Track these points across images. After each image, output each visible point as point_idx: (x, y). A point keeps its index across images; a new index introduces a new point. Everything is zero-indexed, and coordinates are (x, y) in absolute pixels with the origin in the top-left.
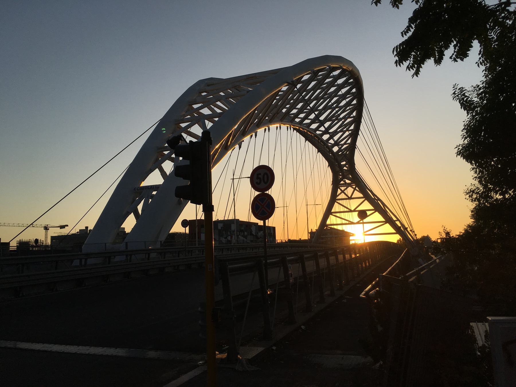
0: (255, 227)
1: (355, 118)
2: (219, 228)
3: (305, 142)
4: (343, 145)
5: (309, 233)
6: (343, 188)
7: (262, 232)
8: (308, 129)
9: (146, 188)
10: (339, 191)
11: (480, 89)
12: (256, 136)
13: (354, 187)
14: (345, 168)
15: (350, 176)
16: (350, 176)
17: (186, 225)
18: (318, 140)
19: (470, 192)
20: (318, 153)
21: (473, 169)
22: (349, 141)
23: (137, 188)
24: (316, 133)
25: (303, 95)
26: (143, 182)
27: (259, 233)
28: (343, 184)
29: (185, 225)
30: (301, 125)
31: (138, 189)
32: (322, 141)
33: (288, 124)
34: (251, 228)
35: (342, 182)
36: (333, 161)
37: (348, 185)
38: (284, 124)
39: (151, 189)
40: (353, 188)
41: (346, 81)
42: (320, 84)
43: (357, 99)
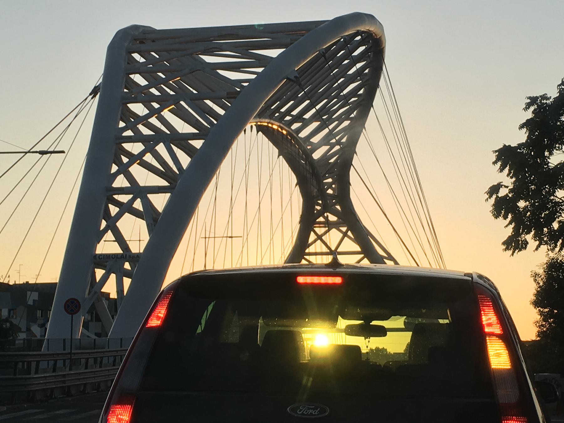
0: (107, 302)
1: (361, 98)
2: (30, 302)
3: (257, 135)
6: (320, 230)
8: (280, 122)
9: (113, 256)
10: (312, 237)
11: (544, 265)
13: (344, 229)
14: (330, 191)
15: (338, 207)
16: (338, 207)
18: (291, 140)
19: (536, 322)
20: (278, 157)
22: (344, 140)
23: (99, 257)
25: (303, 92)
26: (98, 245)
27: (115, 317)
28: (320, 223)
30: (271, 119)
32: (297, 140)
35: (321, 219)
36: (308, 175)
37: (329, 225)
39: (122, 259)
41: (362, 54)
43: (369, 69)
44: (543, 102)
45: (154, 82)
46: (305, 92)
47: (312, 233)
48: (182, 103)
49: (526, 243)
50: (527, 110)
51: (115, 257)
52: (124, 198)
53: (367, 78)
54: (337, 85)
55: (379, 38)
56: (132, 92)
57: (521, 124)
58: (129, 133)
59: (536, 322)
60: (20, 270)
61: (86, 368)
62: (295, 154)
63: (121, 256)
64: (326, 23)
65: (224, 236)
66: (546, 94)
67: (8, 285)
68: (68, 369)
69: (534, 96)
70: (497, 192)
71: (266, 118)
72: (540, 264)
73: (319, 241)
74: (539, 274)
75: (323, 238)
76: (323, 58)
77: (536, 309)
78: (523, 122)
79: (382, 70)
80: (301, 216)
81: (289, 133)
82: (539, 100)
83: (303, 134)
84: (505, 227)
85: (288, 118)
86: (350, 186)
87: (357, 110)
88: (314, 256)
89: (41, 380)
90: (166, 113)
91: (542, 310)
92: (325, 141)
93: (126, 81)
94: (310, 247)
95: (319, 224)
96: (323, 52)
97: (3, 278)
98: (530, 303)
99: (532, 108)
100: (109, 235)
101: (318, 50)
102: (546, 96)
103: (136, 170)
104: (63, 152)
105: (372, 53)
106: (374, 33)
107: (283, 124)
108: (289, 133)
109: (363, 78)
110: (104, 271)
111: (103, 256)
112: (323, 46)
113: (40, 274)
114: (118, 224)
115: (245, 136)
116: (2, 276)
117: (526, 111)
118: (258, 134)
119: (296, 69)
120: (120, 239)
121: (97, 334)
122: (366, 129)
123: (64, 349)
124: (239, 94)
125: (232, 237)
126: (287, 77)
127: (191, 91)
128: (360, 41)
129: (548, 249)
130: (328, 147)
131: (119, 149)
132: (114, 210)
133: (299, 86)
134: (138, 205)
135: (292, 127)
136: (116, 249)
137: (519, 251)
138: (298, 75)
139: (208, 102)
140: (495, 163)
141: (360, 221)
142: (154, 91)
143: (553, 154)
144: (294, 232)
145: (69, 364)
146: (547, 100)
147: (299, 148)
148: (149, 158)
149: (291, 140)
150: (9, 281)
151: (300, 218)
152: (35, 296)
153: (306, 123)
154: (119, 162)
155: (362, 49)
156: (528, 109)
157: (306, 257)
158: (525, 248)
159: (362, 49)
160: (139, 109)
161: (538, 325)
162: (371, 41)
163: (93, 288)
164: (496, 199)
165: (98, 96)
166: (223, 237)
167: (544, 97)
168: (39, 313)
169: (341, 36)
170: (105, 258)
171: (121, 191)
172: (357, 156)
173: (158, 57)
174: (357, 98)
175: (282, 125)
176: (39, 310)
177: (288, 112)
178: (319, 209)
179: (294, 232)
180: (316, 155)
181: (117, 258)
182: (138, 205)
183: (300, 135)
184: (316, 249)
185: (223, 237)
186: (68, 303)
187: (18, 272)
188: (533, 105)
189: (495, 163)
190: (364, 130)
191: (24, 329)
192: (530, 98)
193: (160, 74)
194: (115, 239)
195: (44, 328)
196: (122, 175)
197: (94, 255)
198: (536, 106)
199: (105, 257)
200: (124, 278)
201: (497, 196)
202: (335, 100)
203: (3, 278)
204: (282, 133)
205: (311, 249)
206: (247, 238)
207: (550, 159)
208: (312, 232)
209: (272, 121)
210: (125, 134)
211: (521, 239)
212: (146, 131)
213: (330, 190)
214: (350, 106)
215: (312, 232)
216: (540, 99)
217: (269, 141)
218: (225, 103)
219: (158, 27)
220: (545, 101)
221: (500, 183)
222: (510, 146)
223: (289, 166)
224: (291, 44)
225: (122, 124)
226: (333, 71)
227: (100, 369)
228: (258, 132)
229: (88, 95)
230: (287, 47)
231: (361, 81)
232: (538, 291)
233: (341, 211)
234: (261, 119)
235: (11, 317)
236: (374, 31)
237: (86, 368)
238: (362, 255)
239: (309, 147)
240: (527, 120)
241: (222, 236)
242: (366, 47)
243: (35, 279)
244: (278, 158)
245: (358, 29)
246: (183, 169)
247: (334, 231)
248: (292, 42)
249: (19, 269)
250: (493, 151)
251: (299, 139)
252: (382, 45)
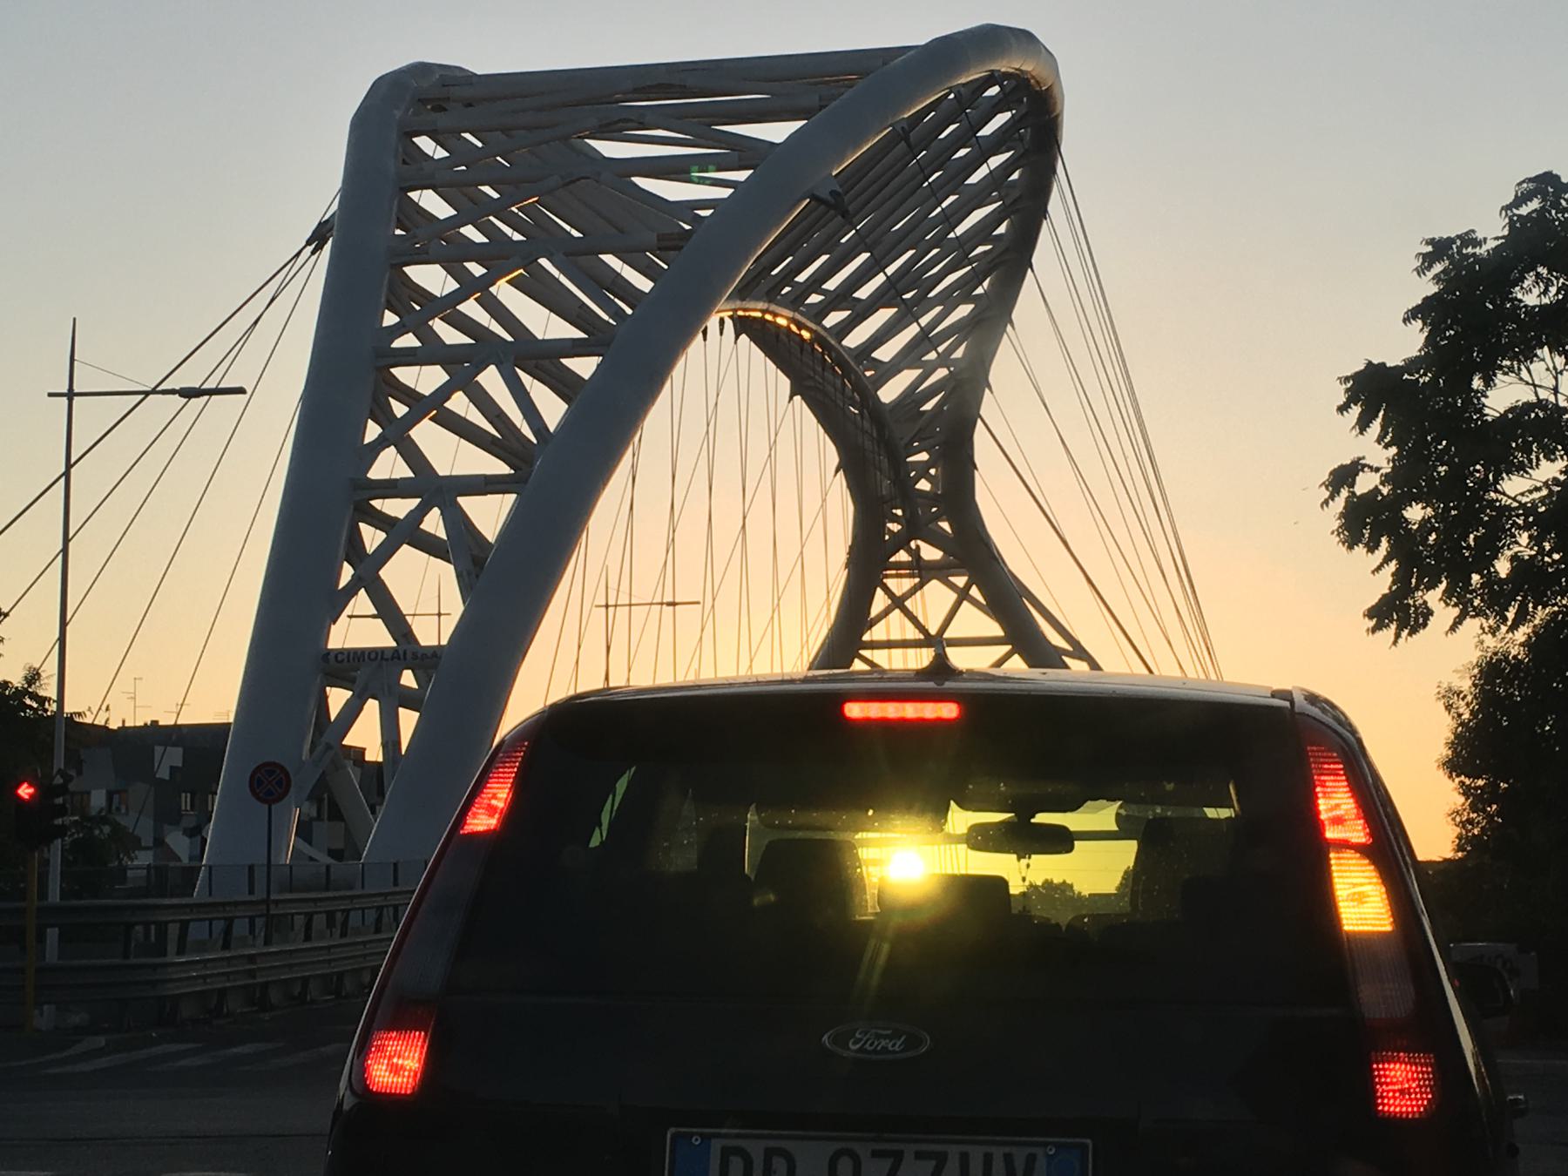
0: (358, 770)
2: (163, 773)
3: (736, 343)
4: (929, 370)
6: (899, 585)
8: (795, 310)
9: (373, 656)
10: (880, 601)
11: (1473, 669)
13: (960, 581)
14: (924, 485)
15: (945, 525)
16: (945, 525)
18: (823, 354)
19: (1452, 814)
20: (791, 398)
21: (1456, 789)
23: (336, 657)
24: (824, 328)
25: (854, 231)
26: (333, 628)
27: (378, 808)
28: (899, 566)
30: (770, 301)
35: (902, 556)
36: (868, 444)
37: (923, 572)
39: (395, 660)
40: (952, 586)
42: (933, 198)
44: (1464, 251)
45: (472, 210)
46: (857, 231)
47: (879, 592)
48: (544, 262)
49: (1428, 613)
50: (1424, 274)
52: (398, 508)
53: (1016, 194)
54: (940, 212)
55: (1047, 89)
56: (415, 237)
57: (1410, 308)
58: (408, 341)
59: (1452, 814)
60: (135, 693)
61: (308, 938)
62: (833, 390)
63: (394, 654)
64: (909, 54)
65: (654, 601)
66: (1473, 231)
67: (105, 728)
68: (261, 941)
69: (1442, 238)
70: (1352, 485)
71: (758, 299)
72: (1463, 665)
73: (897, 611)
74: (1462, 692)
75: (908, 603)
76: (903, 142)
77: (1453, 780)
78: (1414, 305)
79: (1054, 172)
80: (853, 551)
81: (817, 337)
82: (1454, 246)
83: (854, 340)
84: (1373, 572)
85: (815, 298)
86: (976, 472)
87: (992, 276)
88: (885, 651)
89: (195, 971)
90: (503, 291)
91: (1467, 782)
92: (909, 357)
93: (400, 208)
94: (874, 629)
95: (897, 570)
96: (903, 128)
97: (92, 713)
98: (1437, 764)
99: (1438, 268)
100: (362, 602)
101: (889, 123)
102: (1474, 237)
103: (426, 434)
104: (241, 391)
105: (1029, 130)
106: (1033, 77)
107: (802, 313)
108: (817, 337)
109: (1007, 195)
110: (351, 693)
111: (346, 653)
112: (904, 114)
113: (186, 702)
114: (384, 573)
116: (90, 708)
117: (1422, 275)
118: (738, 341)
119: (834, 174)
120: (388, 610)
121: (332, 853)
122: (1015, 326)
123: (251, 892)
124: (688, 240)
125: (673, 604)
126: (813, 195)
127: (567, 231)
128: (996, 100)
129: (1482, 628)
130: (919, 371)
131: (384, 381)
132: (372, 537)
133: (843, 217)
134: (434, 523)
135: (824, 322)
136: (378, 636)
137: (1410, 634)
138: (841, 186)
139: (610, 260)
140: (1343, 409)
141: (1000, 561)
142: (470, 232)
143: (1495, 385)
144: (834, 589)
145: (264, 929)
146: (1474, 247)
147: (843, 376)
148: (459, 403)
149: (823, 354)
150: (108, 720)
151: (849, 553)
152: (175, 756)
153: (863, 312)
154: (383, 415)
155: (1002, 119)
156: (1429, 271)
157: (862, 652)
158: (1425, 625)
159: (1002, 119)
160: (432, 278)
161: (1458, 819)
162: (1025, 99)
163: (321, 734)
164: (1347, 499)
165: (328, 247)
166: (651, 604)
167: (1468, 239)
168: (185, 800)
169: (950, 85)
171: (392, 488)
172: (991, 395)
173: (479, 144)
174: (989, 247)
175: (798, 317)
176: (186, 792)
177: (815, 284)
178: (896, 531)
179: (834, 589)
180: (889, 393)
181: (382, 658)
182: (434, 523)
183: (845, 343)
184: (888, 632)
185: (651, 604)
186: (259, 775)
187: (132, 698)
188: (1440, 259)
189: (1343, 409)
190: (1009, 328)
191: (148, 840)
192: (1431, 242)
193: (487, 189)
194: (375, 612)
195: (199, 838)
196: (393, 447)
197: (325, 652)
198: (1447, 262)
200: (401, 710)
201: (1349, 491)
202: (935, 251)
203: (92, 713)
204: (800, 336)
205: (877, 633)
206: (713, 606)
207: (1486, 397)
208: (879, 590)
209: (773, 307)
210: (398, 343)
211: (1415, 602)
212: (450, 336)
213: (923, 480)
214: (974, 265)
215: (879, 590)
216: (1459, 242)
217: (767, 358)
218: (654, 261)
219: (480, 68)
220: (1470, 250)
221: (1360, 459)
222: (1383, 364)
223: (819, 421)
224: (821, 108)
225: (390, 319)
226: (930, 177)
227: (344, 941)
228: (737, 338)
229: (304, 243)
230: (811, 118)
231: (1001, 202)
232: (1457, 736)
233: (953, 536)
234: (744, 303)
235: (114, 807)
236: (1034, 74)
237: (308, 938)
238: (1008, 648)
239: (868, 374)
240: (1426, 299)
241: (649, 602)
242: (1013, 115)
243: (175, 715)
244: (789, 402)
245: (992, 68)
246: (548, 430)
247: (934, 586)
248: (823, 103)
249: (133, 691)
250: (1340, 378)
251: (843, 353)
252: (1054, 110)
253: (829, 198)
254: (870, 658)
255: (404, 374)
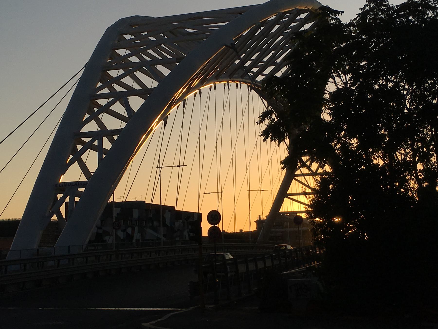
5: (255, 221)
7: (181, 221)
12: (184, 105)
17: (118, 227)
23: (59, 186)
26: (62, 176)
29: (116, 227)
31: (60, 186)
33: (225, 79)
34: (164, 216)
38: (219, 82)
51: (70, 186)
65: (174, 166)
103: (105, 118)
115: (215, 91)
152: (118, 210)
157: (296, 178)
170: (64, 186)
171: (87, 135)
181: (72, 185)
199: (64, 186)
209: (244, 80)
212: (119, 89)
225: (100, 84)
234: (231, 79)
241: (172, 165)
253: (231, 46)
254: (297, 179)
255: (99, 101)
